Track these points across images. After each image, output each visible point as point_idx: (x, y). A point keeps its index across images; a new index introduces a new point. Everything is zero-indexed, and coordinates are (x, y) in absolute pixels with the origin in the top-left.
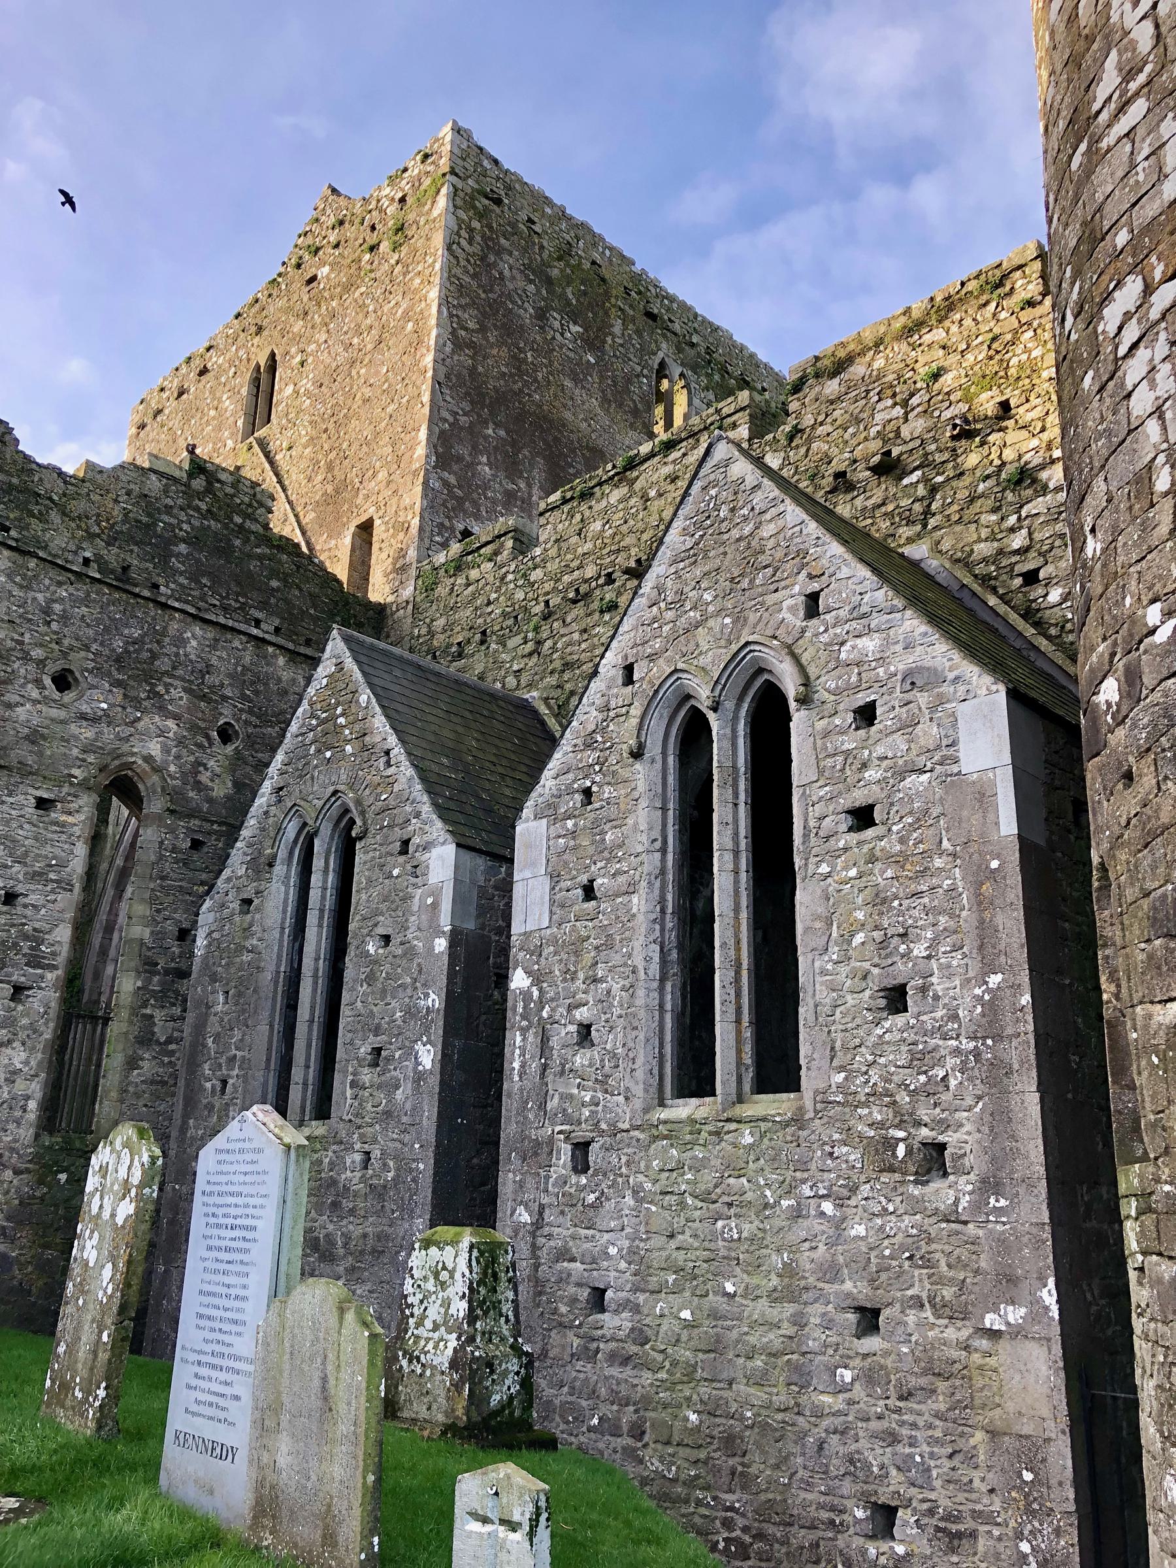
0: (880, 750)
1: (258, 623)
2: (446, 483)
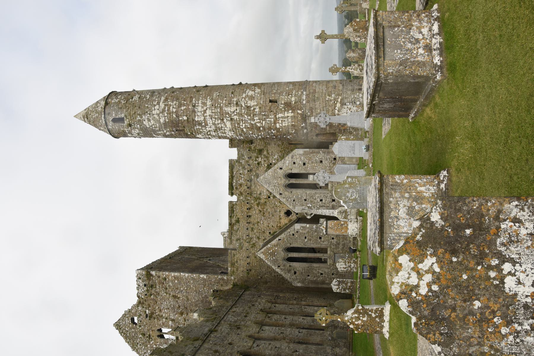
0: (298, 162)
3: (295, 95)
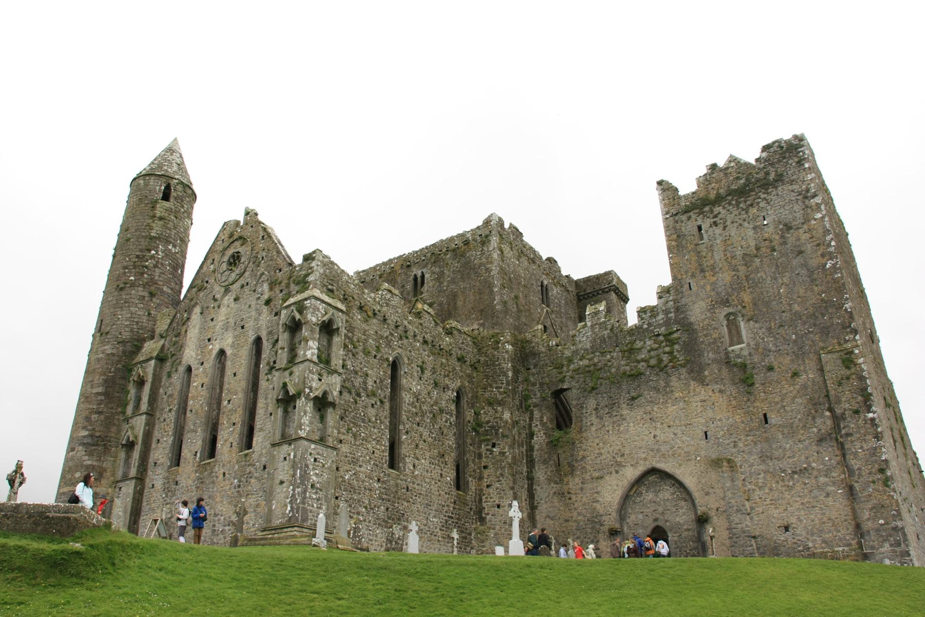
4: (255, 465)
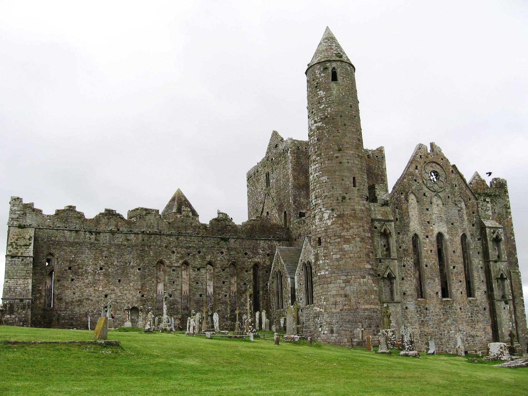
1: (270, 237)
2: (295, 206)
3: (324, 263)
4: (479, 307)
